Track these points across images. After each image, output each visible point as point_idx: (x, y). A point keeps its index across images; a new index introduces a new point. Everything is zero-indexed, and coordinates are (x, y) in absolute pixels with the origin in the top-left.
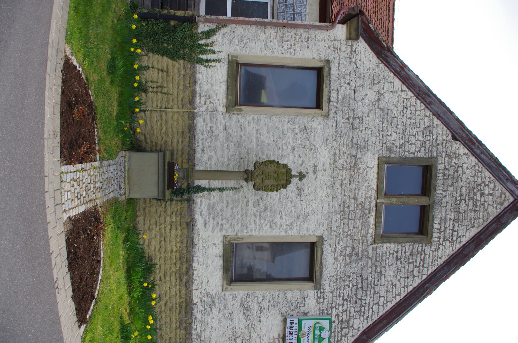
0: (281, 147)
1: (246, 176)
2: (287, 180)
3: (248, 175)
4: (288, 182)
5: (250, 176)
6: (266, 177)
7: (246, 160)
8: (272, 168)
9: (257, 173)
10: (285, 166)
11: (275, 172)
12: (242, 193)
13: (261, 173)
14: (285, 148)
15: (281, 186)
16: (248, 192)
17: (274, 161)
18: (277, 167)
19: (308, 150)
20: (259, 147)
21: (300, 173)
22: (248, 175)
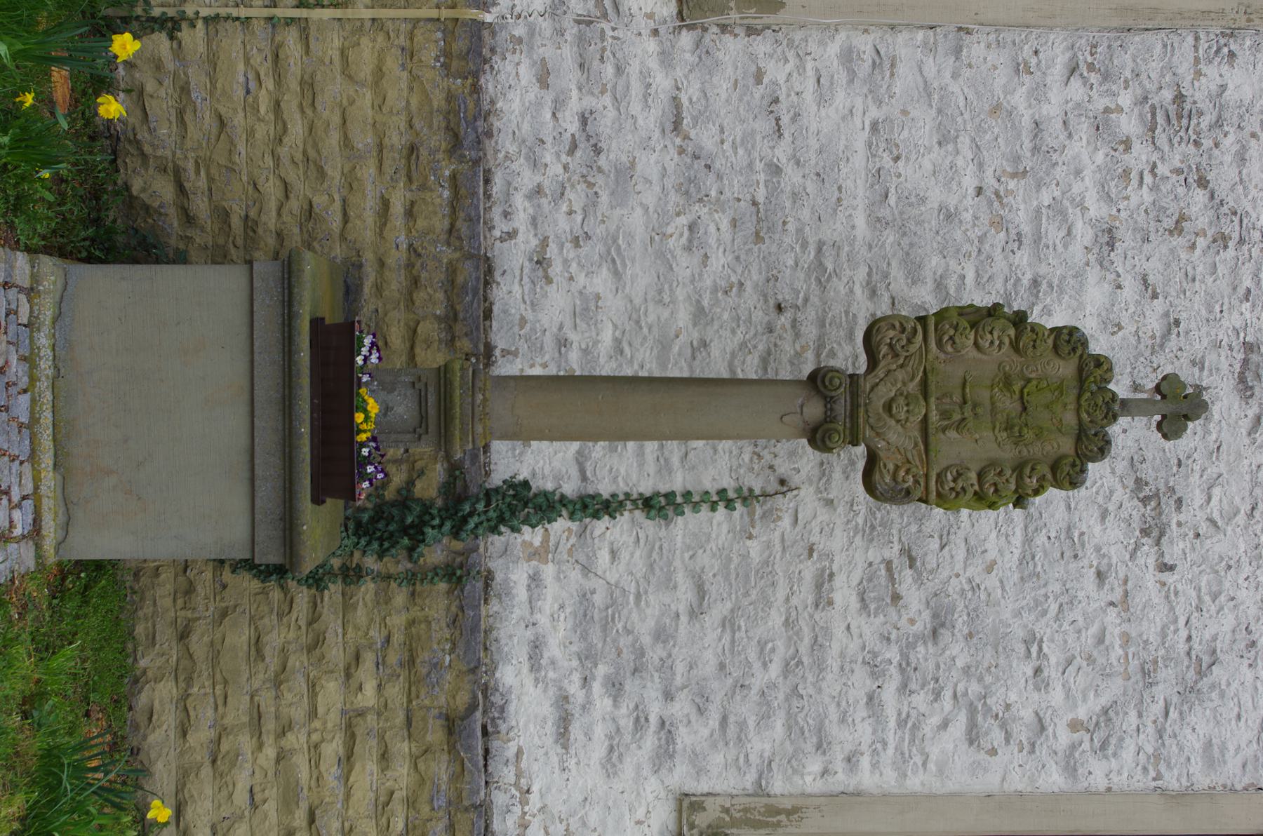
0: (1026, 229)
1: (814, 410)
2: (1081, 435)
3: (828, 400)
4: (1092, 444)
5: (841, 408)
6: (945, 415)
7: (811, 313)
8: (982, 359)
9: (886, 392)
10: (1069, 340)
11: (1007, 382)
12: (786, 522)
13: (913, 387)
14: (1054, 233)
15: (1044, 469)
16: (823, 515)
17: (993, 311)
18: (1015, 346)
19: (1202, 243)
20: (890, 237)
21: (1168, 388)
22: (828, 400)
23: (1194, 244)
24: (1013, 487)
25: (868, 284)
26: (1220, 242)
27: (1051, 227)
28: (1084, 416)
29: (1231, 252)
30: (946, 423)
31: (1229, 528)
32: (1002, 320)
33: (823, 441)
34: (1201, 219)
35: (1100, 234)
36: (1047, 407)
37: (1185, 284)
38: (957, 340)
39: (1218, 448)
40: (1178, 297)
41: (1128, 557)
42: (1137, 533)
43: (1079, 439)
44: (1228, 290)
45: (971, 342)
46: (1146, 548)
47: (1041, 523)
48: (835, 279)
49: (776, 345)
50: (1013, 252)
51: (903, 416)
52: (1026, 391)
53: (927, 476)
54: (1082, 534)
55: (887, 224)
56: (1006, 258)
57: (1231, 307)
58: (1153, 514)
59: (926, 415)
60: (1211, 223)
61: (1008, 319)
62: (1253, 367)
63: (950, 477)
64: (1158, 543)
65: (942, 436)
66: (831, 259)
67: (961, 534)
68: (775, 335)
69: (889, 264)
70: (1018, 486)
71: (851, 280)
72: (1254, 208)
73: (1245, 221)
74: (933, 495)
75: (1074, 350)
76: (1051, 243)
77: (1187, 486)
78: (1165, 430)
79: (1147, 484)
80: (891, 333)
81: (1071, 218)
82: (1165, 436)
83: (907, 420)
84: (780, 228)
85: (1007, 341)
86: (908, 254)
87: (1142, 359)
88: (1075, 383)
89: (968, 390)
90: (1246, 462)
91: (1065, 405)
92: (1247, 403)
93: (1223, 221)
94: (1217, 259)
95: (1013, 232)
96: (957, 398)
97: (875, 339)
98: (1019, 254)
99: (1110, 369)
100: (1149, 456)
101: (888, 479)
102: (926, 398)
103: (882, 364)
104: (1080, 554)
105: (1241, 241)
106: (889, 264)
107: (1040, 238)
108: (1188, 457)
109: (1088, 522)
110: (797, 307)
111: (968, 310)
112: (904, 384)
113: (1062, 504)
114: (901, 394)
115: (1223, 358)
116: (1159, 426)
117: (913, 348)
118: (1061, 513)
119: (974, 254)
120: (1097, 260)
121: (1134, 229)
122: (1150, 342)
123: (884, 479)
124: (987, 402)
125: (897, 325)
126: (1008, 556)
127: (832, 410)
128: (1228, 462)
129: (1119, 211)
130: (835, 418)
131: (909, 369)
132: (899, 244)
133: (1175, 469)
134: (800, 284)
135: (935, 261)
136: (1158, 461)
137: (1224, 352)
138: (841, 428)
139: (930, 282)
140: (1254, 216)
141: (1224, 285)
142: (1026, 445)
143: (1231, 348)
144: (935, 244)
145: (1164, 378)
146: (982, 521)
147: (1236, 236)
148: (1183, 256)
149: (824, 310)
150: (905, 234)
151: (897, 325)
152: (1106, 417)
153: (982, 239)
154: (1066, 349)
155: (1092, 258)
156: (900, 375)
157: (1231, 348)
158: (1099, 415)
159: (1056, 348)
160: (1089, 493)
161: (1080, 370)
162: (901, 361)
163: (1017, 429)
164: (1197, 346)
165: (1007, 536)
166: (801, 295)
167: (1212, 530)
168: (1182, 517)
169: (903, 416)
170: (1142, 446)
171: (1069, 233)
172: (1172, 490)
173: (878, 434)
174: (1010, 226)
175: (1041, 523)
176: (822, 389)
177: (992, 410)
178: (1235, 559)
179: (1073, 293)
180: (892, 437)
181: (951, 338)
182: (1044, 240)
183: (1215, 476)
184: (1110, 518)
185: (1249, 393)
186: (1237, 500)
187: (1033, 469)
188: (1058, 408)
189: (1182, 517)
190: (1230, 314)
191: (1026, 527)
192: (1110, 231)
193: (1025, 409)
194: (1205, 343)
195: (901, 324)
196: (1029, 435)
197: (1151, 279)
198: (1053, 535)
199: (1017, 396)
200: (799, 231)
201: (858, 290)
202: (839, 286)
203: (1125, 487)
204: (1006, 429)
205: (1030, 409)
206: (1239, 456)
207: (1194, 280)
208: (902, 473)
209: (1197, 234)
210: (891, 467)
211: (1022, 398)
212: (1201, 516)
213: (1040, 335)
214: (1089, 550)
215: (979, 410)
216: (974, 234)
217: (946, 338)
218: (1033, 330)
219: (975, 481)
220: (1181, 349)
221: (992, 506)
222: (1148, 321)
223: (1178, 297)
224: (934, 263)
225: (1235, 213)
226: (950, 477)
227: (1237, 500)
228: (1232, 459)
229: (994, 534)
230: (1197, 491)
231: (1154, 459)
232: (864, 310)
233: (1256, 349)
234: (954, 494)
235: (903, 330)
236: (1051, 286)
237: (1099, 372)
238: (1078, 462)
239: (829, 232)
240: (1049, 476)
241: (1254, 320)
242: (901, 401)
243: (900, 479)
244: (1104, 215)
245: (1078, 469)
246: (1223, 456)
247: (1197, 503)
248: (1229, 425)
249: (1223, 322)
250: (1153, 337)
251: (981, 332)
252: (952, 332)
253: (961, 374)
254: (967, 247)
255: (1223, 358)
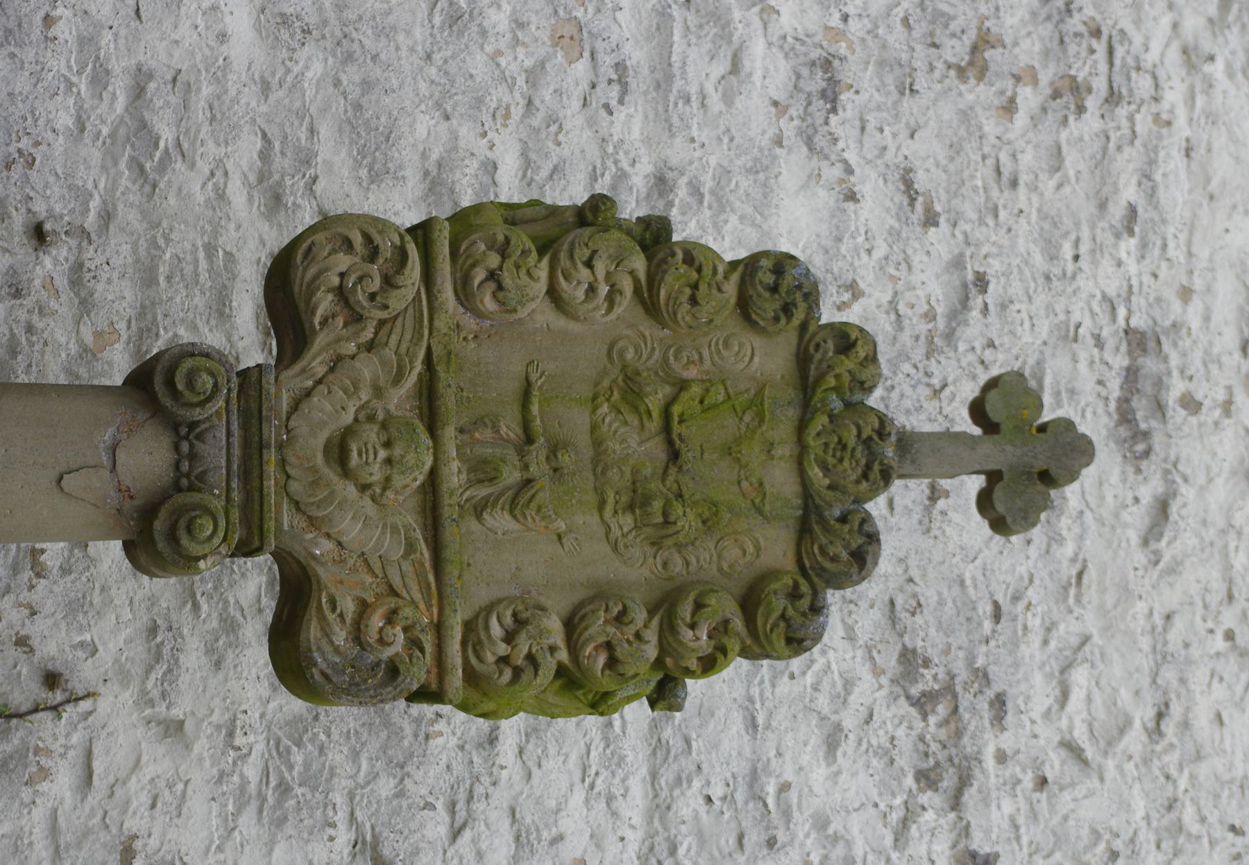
0: (638, 55)
1: (147, 458)
2: (808, 520)
3: (184, 433)
4: (833, 547)
5: (218, 453)
6: (482, 471)
7: (118, 251)
8: (567, 334)
9: (329, 413)
10: (773, 287)
11: (631, 390)
12: (63, 782)
13: (400, 399)
14: (700, 68)
15: (725, 606)
16: (159, 762)
17: (595, 212)
18: (648, 299)
19: (1028, 99)
20: (314, 64)
21: (1003, 408)
22: (184, 433)
23: (1012, 100)
24: (652, 652)
25: (261, 178)
26: (1068, 98)
27: (693, 54)
28: (815, 473)
29: (1091, 122)
30: (482, 492)
31: (1110, 764)
32: (616, 234)
33: (173, 538)
34: (1025, 44)
35: (805, 72)
36: (728, 451)
37: (995, 193)
38: (507, 281)
39: (1080, 575)
40: (981, 222)
41: (889, 840)
42: (909, 781)
43: (804, 530)
44: (1087, 209)
45: (542, 286)
46: (929, 816)
47: (688, 764)
48: (179, 165)
49: (30, 329)
50: (607, 107)
51: (376, 474)
52: (676, 410)
53: (439, 628)
54: (784, 788)
55: (306, 31)
56: (591, 122)
57: (1097, 249)
58: (943, 734)
59: (433, 473)
60: (1046, 53)
61: (629, 233)
62: (1147, 386)
63: (496, 630)
64: (956, 804)
65: (474, 525)
66: (168, 114)
67: (501, 798)
68: (28, 302)
69: (312, 131)
70: (663, 650)
71: (219, 168)
72: (1138, 22)
73: (1119, 52)
74: (456, 679)
75: (787, 309)
76: (693, 90)
77: (1016, 665)
78: (1000, 508)
79: (927, 663)
80: (343, 261)
81: (739, 31)
82: (1000, 525)
83: (387, 483)
84: (36, 34)
85: (627, 285)
86: (358, 107)
87: (907, 367)
88: (791, 393)
89: (535, 409)
90: (1141, 607)
91: (769, 447)
92: (1138, 471)
93: (1072, 49)
94: (1064, 135)
95: (607, 61)
96: (510, 428)
97: (301, 276)
98: (621, 114)
99: (872, 359)
100: (929, 596)
101: (341, 637)
102: (433, 429)
103: (321, 340)
104: (782, 837)
105: (1113, 98)
106: (312, 131)
107: (669, 78)
108: (1016, 598)
109: (797, 757)
110: (85, 234)
111: (529, 212)
112: (378, 392)
113: (737, 718)
114: (371, 418)
115: (1083, 367)
116: (985, 501)
117: (400, 300)
118: (733, 736)
119: (517, 112)
120: (800, 133)
121: (881, 64)
122: (923, 328)
123: (328, 639)
124: (583, 439)
125: (358, 240)
126: (613, 848)
127: (193, 457)
128: (1102, 611)
129: (845, 18)
130: (201, 477)
131: (389, 353)
132: (337, 83)
133: (987, 626)
134: (91, 176)
135: (424, 124)
136: (949, 609)
137: (1086, 351)
138: (218, 505)
139: (412, 174)
140: (1138, 40)
141: (1078, 198)
142: (679, 547)
143: (1099, 342)
144: (423, 87)
145: (992, 384)
146: (549, 765)
147: (1100, 84)
148: (991, 128)
149: (153, 243)
150: (349, 58)
151: (358, 240)
152: (865, 476)
153: (534, 76)
154: (768, 306)
155: (789, 128)
156: (367, 368)
157: (1099, 342)
158: (850, 471)
159: (744, 305)
160: (797, 687)
161: (803, 359)
162: (368, 334)
163: (657, 505)
164: (1027, 338)
165: (610, 799)
166: (95, 203)
167: (1073, 769)
168: (1007, 741)
169: (376, 474)
170: (914, 572)
171: (735, 67)
172: (983, 676)
173: (313, 522)
174: (599, 45)
175: (688, 764)
176: (167, 401)
177: (596, 461)
178: (1126, 835)
179: (749, 210)
180: (350, 529)
181: (492, 275)
182: (678, 84)
183: (1075, 641)
184: (847, 747)
185: (1140, 447)
186: (1125, 696)
187: (699, 606)
188: (753, 452)
189: (1007, 741)
190: (1095, 263)
191: (654, 776)
192: (827, 64)
193: (674, 455)
194: (1044, 329)
195: (368, 239)
196: (687, 521)
197: (921, 181)
198: (717, 792)
199: (655, 424)
200: (87, 42)
201: (237, 193)
202: (189, 184)
203: (877, 671)
204: (631, 507)
205: (687, 455)
206: (1126, 594)
207: (1014, 184)
208: (376, 621)
209: (1017, 79)
210: (348, 606)
211: (667, 428)
212: (1048, 734)
213: (707, 271)
214: (802, 824)
215: (565, 459)
216: (516, 63)
217: (479, 275)
218: (689, 259)
219: (558, 638)
220: (991, 344)
221: (600, 703)
222: (917, 278)
223: (981, 222)
224: (421, 130)
225: (1097, 33)
226: (496, 630)
227: (1125, 696)
228: (1110, 600)
229: (578, 796)
230: (1038, 678)
231: (941, 603)
232: (252, 244)
233: (1151, 345)
234: (508, 674)
235: (373, 254)
236: (696, 192)
237: (847, 364)
238: (804, 587)
239: (162, 47)
240: (738, 624)
241: (1147, 279)
242: (371, 434)
243: (372, 636)
244: (812, 28)
245: (805, 603)
246: (1091, 593)
247: (1037, 711)
248: (1101, 521)
249: (1081, 281)
250: (930, 316)
251: (564, 261)
252: (494, 260)
253: (518, 368)
254: (499, 94)
255: (1083, 367)
